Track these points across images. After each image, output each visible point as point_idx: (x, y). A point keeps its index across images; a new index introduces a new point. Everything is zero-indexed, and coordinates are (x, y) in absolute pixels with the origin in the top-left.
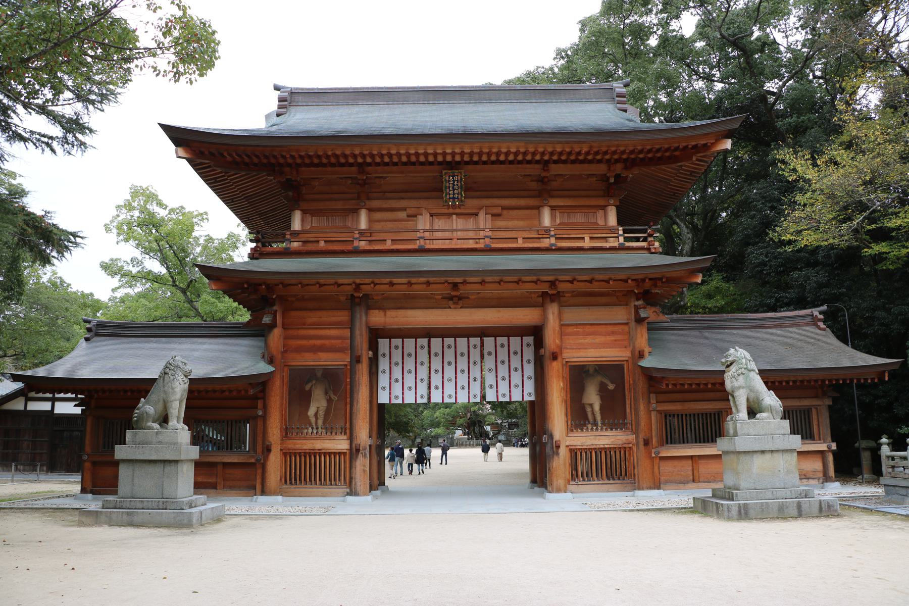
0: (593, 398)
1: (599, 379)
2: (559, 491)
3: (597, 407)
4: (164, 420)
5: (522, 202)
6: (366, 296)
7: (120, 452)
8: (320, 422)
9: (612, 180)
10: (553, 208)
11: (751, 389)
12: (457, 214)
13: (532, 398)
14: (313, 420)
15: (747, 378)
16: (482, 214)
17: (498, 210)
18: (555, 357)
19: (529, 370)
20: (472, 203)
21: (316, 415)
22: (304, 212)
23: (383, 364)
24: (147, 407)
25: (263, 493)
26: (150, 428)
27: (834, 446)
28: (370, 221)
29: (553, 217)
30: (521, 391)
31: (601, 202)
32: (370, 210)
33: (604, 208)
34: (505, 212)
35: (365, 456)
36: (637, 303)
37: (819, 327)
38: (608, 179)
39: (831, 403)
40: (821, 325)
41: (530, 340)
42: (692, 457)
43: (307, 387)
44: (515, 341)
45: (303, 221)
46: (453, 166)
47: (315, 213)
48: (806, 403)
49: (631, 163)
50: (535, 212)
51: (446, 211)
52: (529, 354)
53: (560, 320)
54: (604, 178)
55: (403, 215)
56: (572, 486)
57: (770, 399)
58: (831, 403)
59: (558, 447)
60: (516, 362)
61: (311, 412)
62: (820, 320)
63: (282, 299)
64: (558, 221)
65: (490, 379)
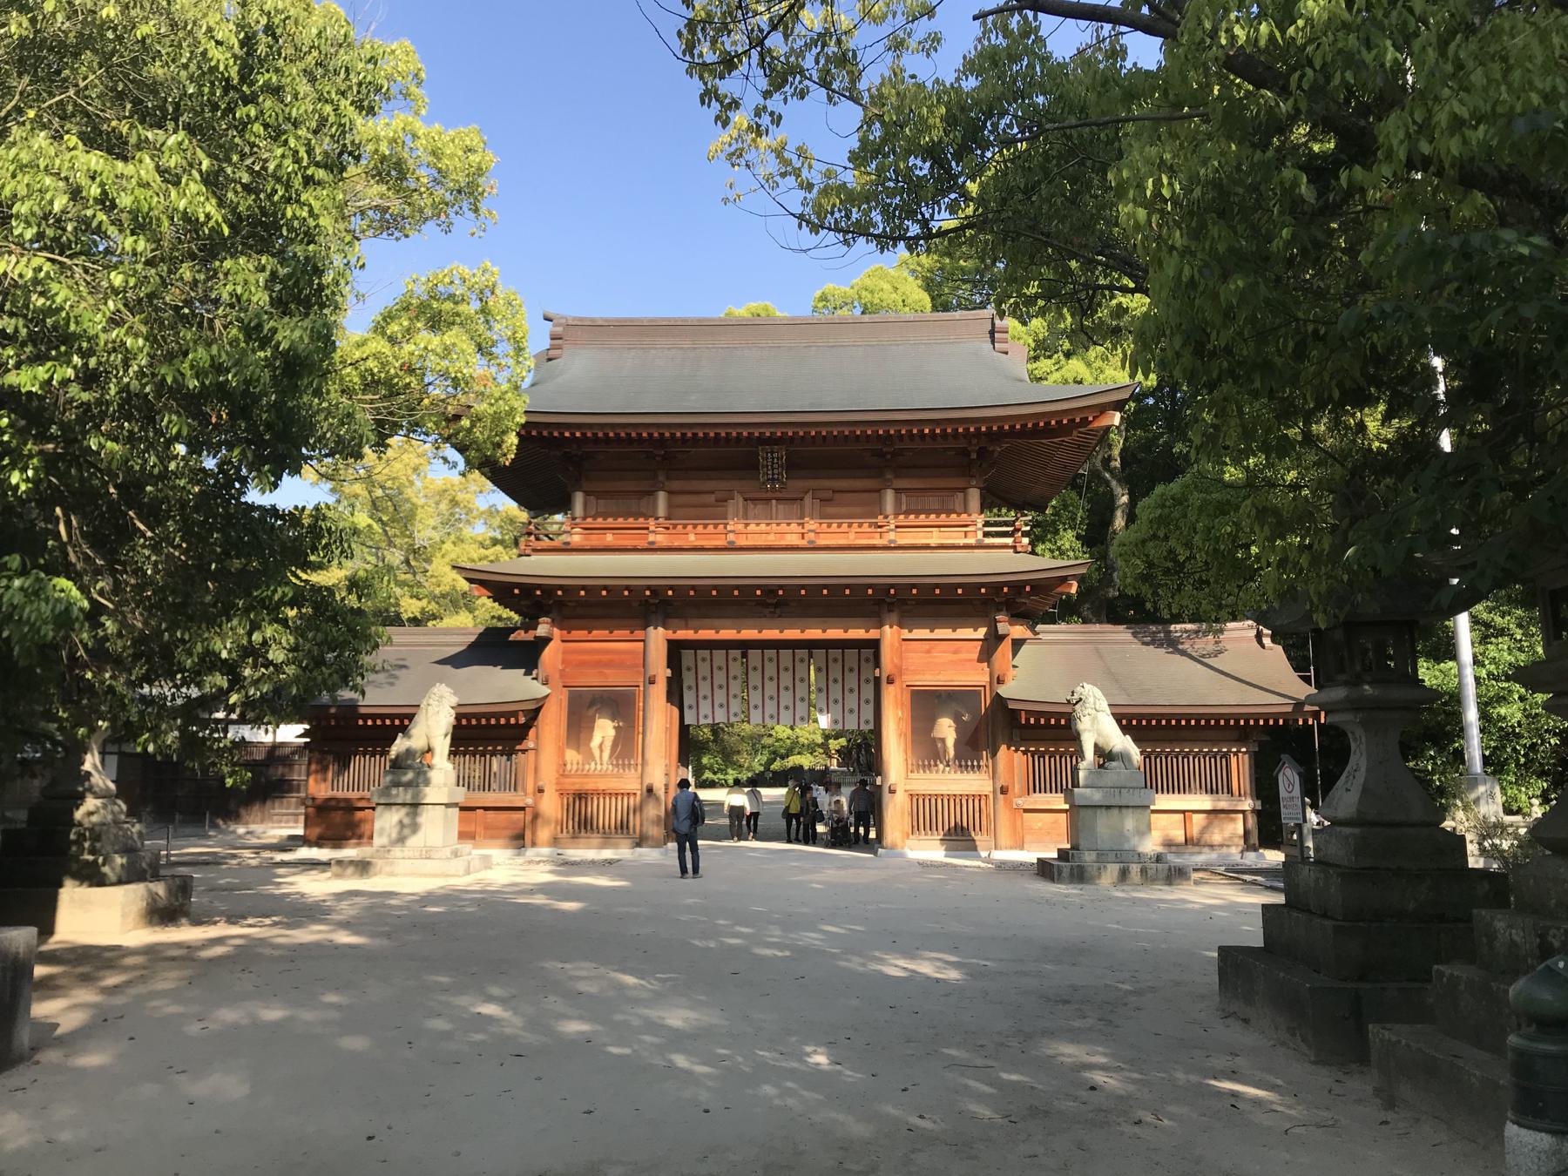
0: (946, 729)
3: (950, 743)
8: (606, 755)
9: (974, 456)
10: (898, 491)
14: (597, 753)
15: (1094, 720)
16: (808, 499)
17: (829, 494)
18: (890, 681)
20: (797, 484)
21: (601, 746)
23: (688, 679)
28: (670, 506)
29: (898, 503)
31: (959, 483)
32: (670, 493)
33: (964, 490)
34: (837, 496)
37: (1263, 646)
38: (968, 454)
46: (772, 441)
47: (599, 495)
50: (875, 495)
51: (764, 496)
54: (965, 453)
55: (711, 498)
59: (892, 792)
61: (595, 743)
64: (904, 508)
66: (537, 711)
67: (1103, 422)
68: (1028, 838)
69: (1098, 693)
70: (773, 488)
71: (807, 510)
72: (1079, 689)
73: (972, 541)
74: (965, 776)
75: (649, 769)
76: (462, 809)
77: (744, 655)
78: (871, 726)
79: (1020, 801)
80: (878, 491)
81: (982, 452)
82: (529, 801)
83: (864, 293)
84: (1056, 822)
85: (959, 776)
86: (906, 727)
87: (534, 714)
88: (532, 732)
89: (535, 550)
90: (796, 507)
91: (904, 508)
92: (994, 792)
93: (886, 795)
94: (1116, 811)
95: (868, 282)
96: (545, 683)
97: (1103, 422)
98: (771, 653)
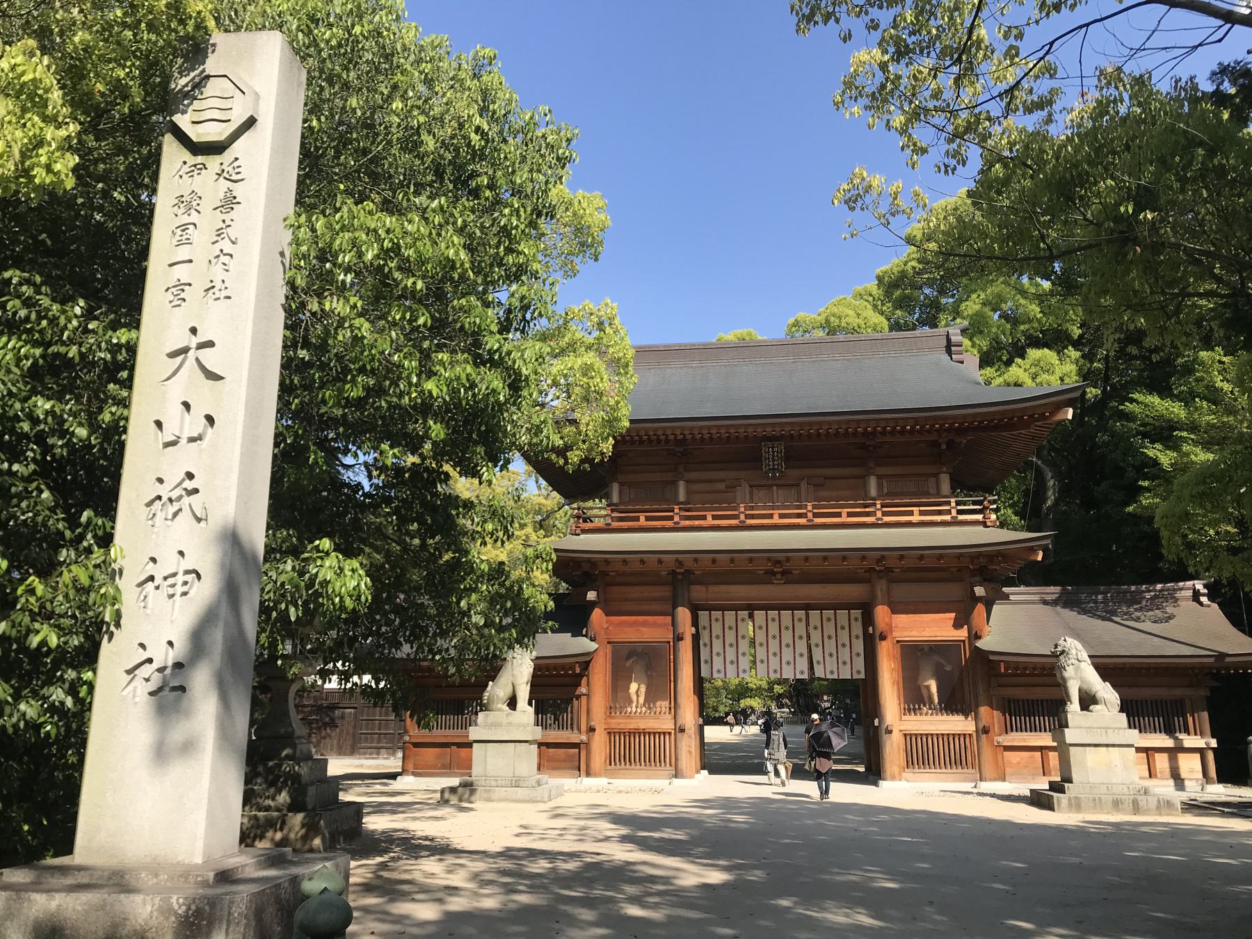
1: (936, 658)
2: (893, 778)
4: (512, 703)
5: (846, 471)
6: (689, 572)
7: (474, 733)
8: (642, 700)
9: (944, 447)
10: (879, 477)
11: (1082, 680)
12: (778, 486)
13: (862, 676)
14: (634, 698)
15: (1077, 669)
16: (803, 486)
18: (883, 638)
19: (859, 646)
22: (621, 484)
23: (705, 638)
24: (497, 691)
25: (588, 774)
26: (500, 710)
27: (1214, 743)
28: (689, 493)
29: (880, 487)
30: (848, 668)
32: (687, 481)
33: (936, 475)
35: (690, 737)
36: (973, 580)
37: (1201, 604)
39: (1208, 694)
40: (1204, 599)
41: (857, 613)
42: (1041, 749)
43: (628, 664)
44: (843, 614)
45: (620, 493)
48: (1178, 692)
49: (961, 431)
52: (858, 629)
53: (889, 597)
54: (935, 444)
55: (722, 486)
56: (908, 774)
57: (1107, 693)
58: (1208, 694)
59: (890, 732)
60: (844, 637)
62: (1204, 595)
63: (605, 574)
64: (885, 491)
65: (817, 654)
66: (588, 663)
67: (1059, 417)
68: (1008, 771)
69: (1079, 646)
70: (774, 477)
71: (803, 494)
72: (1061, 642)
73: (948, 518)
74: (951, 717)
75: (681, 712)
76: (540, 745)
77: (751, 616)
78: (862, 676)
79: (1000, 739)
80: (863, 477)
81: (950, 444)
82: (584, 738)
83: (832, 319)
84: (1032, 757)
85: (945, 717)
86: (897, 676)
87: (586, 665)
88: (584, 680)
89: (584, 531)
90: (793, 491)
91: (885, 491)
92: (977, 731)
93: (885, 737)
94: (1104, 749)
95: (835, 310)
96: (593, 640)
97: (1059, 417)
98: (773, 614)
